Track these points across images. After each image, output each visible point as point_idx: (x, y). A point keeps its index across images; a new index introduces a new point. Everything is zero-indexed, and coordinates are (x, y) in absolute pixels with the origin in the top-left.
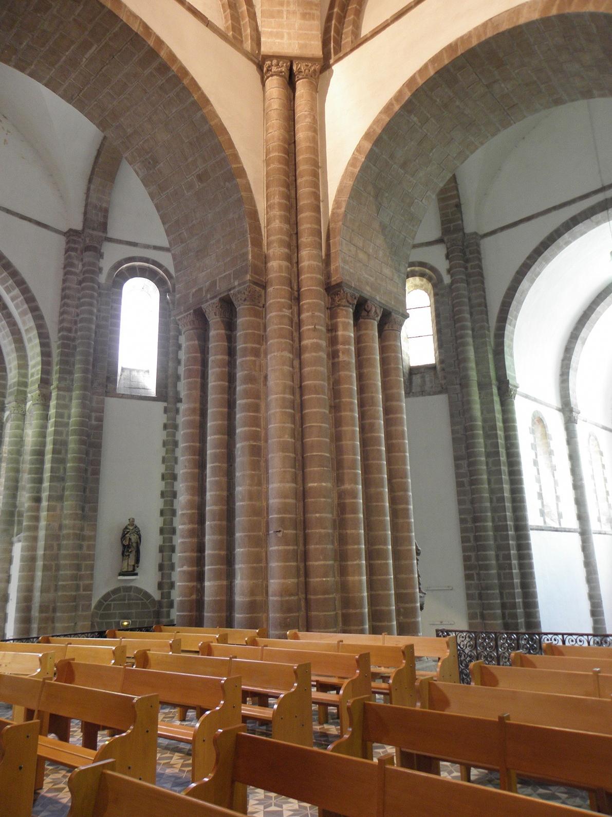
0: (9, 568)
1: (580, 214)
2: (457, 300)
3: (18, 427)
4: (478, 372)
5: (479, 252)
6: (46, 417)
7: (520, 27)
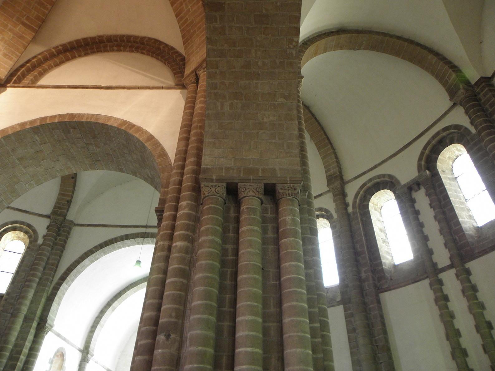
1: (130, 234)
2: (40, 256)
4: (30, 308)
5: (69, 233)
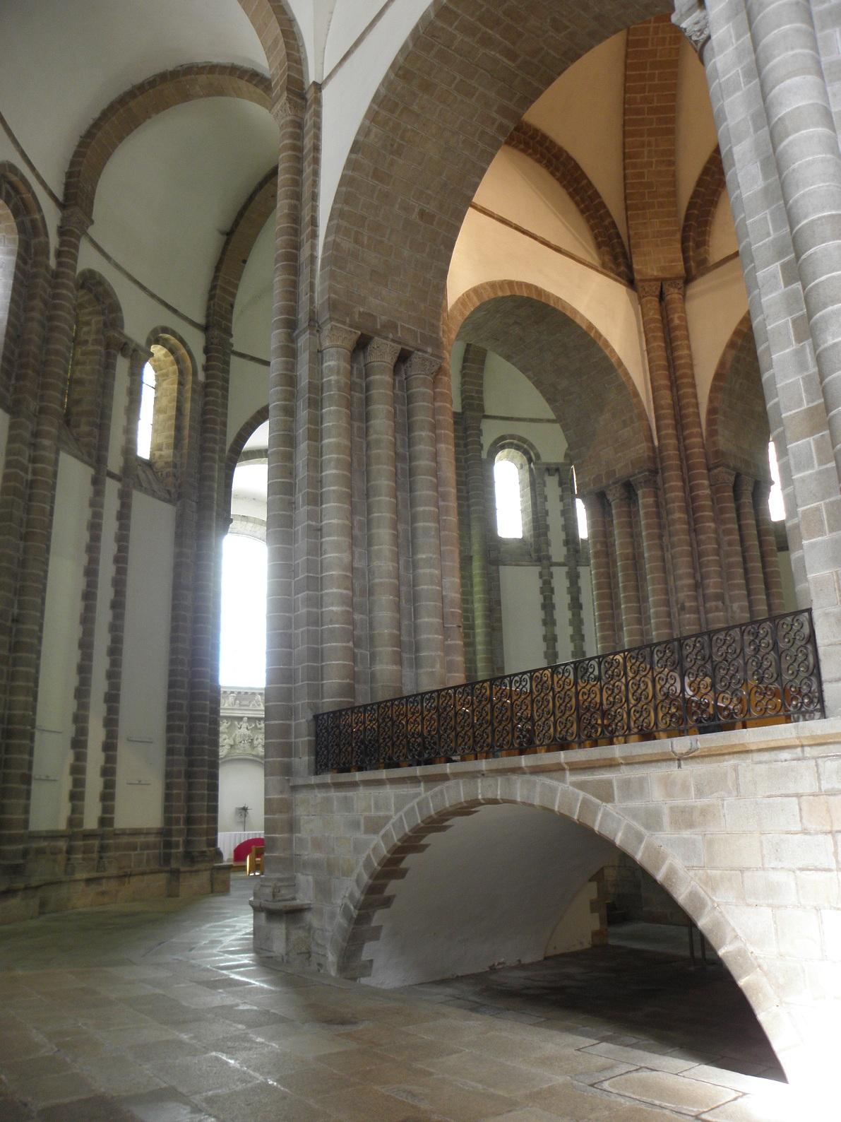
7: (574, 322)
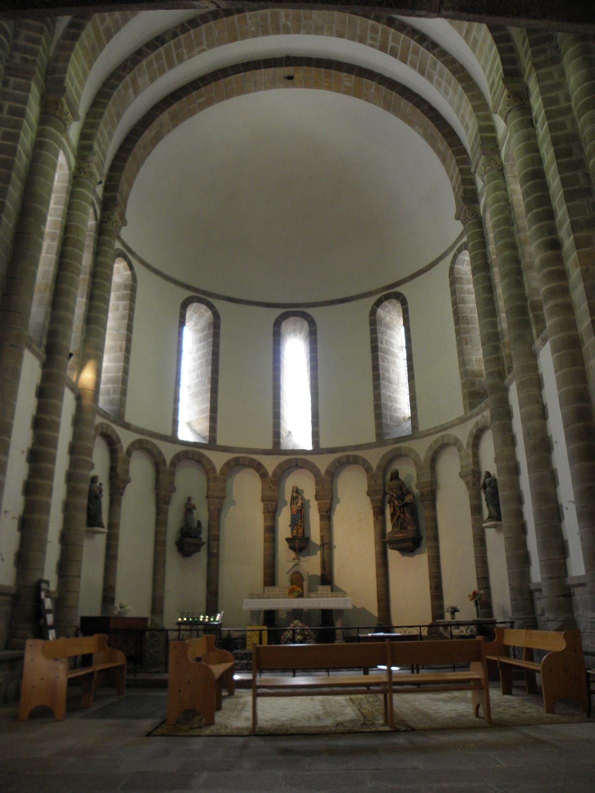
0: (541, 396)
3: (497, 188)
6: (529, 123)
